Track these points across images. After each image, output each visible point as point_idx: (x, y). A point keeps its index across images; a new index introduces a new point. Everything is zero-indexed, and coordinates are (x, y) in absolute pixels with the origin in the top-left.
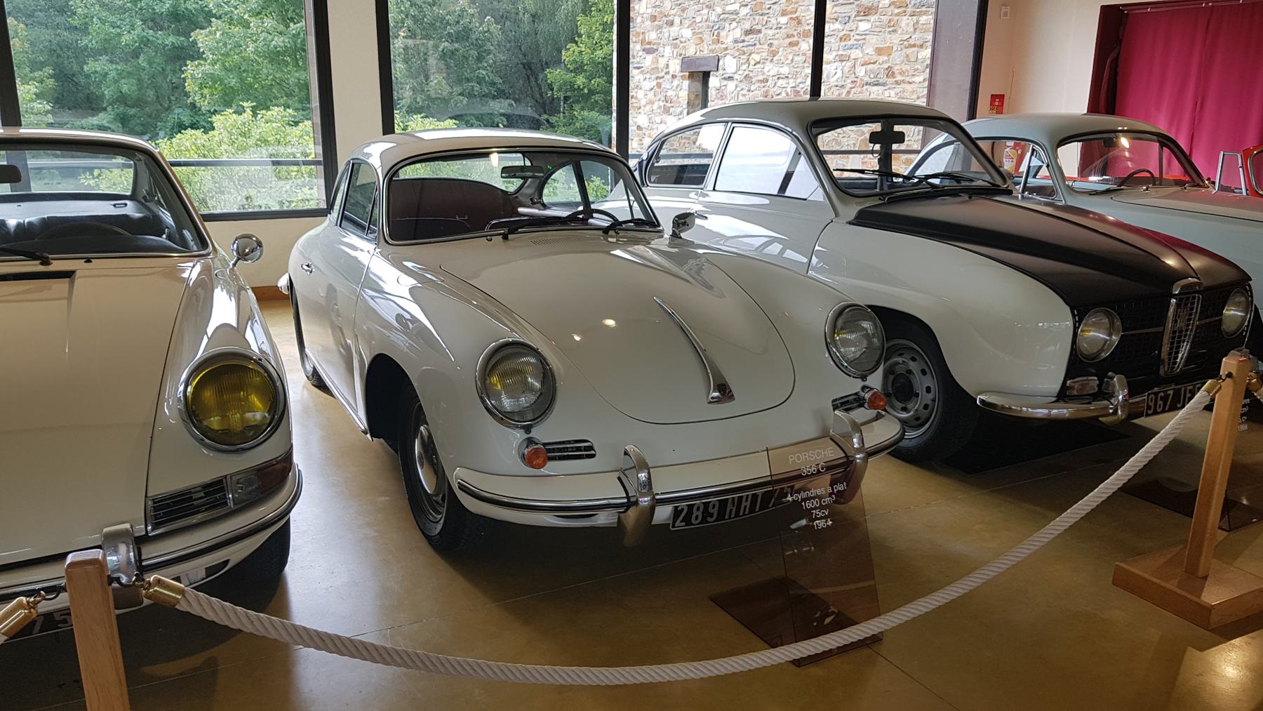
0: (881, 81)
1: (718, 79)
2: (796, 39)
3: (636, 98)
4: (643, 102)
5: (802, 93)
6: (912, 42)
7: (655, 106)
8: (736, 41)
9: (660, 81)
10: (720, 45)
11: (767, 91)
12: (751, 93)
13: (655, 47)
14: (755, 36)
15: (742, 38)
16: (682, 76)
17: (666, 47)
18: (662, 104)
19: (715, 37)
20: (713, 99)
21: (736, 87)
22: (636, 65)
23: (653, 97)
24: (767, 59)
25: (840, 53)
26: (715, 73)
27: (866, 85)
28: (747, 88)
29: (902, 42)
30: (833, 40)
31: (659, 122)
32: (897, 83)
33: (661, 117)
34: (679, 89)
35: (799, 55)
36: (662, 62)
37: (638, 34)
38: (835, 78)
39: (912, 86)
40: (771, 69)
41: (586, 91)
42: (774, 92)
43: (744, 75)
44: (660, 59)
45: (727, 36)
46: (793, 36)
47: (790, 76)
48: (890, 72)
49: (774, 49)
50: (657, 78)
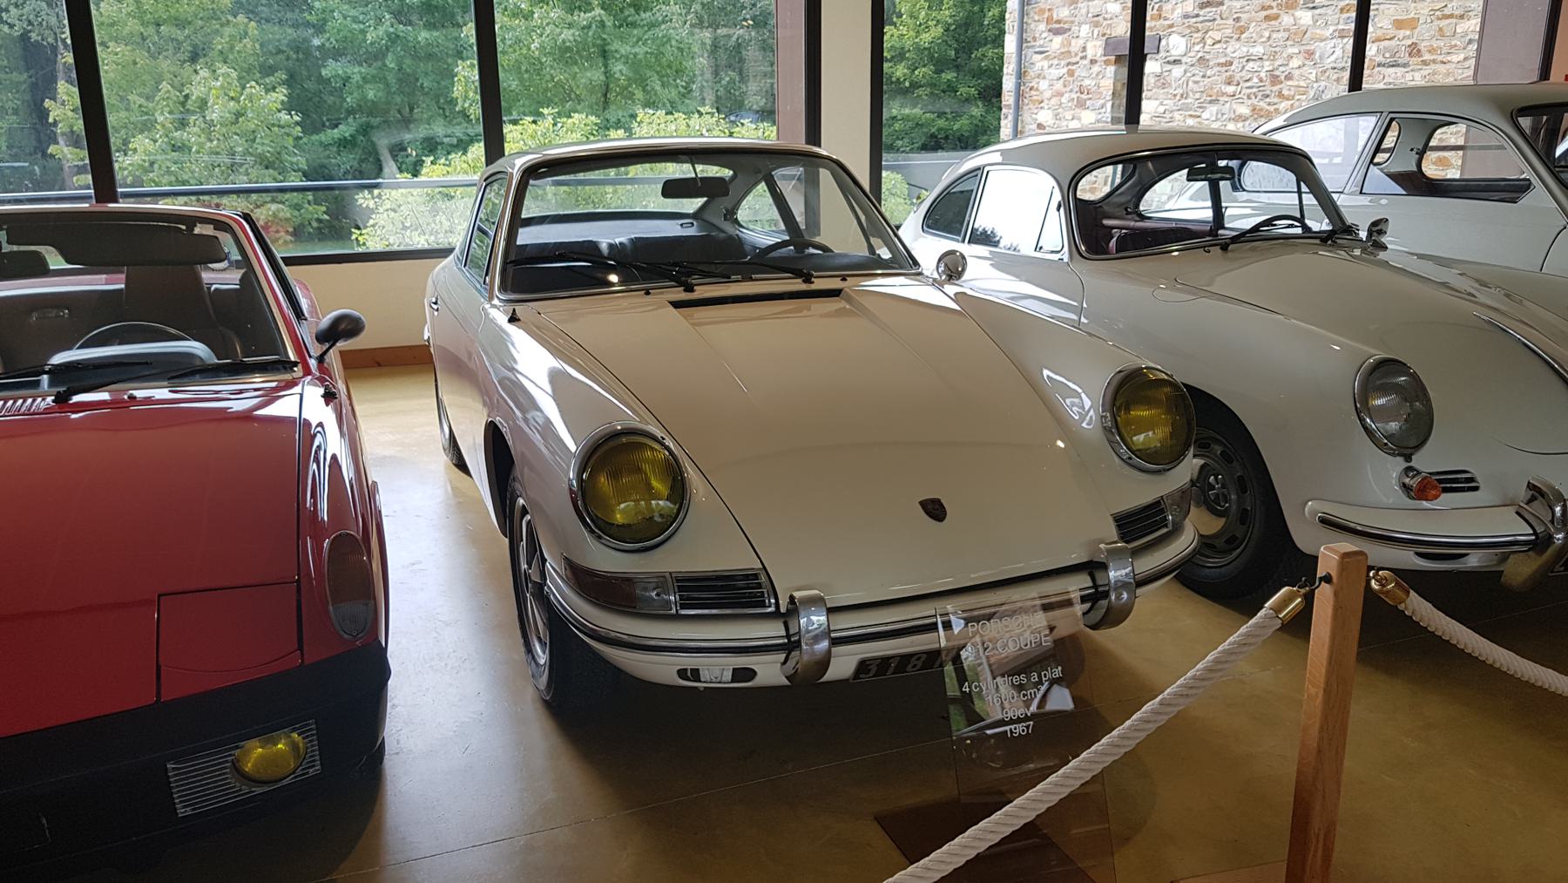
0: (1400, 61)
1: (1158, 64)
2: (1275, 11)
3: (1037, 90)
4: (1048, 94)
5: (1283, 78)
6: (1447, 11)
7: (1063, 100)
8: (1186, 16)
9: (1074, 67)
10: (1161, 21)
11: (1231, 77)
12: (1206, 80)
13: (1066, 26)
14: (1214, 9)
15: (1196, 12)
16: (1105, 62)
17: (1083, 26)
18: (1074, 96)
19: (1155, 11)
20: (1150, 88)
21: (1185, 72)
22: (1037, 50)
23: (1062, 87)
24: (1232, 37)
25: (1341, 27)
26: (1154, 56)
27: (1379, 65)
28: (1201, 74)
29: (1432, 13)
30: (1330, 11)
31: (1070, 118)
32: (1425, 63)
33: (1072, 112)
34: (1100, 77)
35: (1278, 31)
36: (1076, 45)
37: (1042, 11)
38: (1333, 58)
39: (1447, 66)
40: (1236, 49)
41: (907, 84)
42: (1241, 77)
43: (1199, 56)
44: (1074, 42)
45: (1173, 10)
46: (1271, 7)
47: (1265, 57)
48: (1414, 50)
49: (1242, 24)
50: (1068, 64)
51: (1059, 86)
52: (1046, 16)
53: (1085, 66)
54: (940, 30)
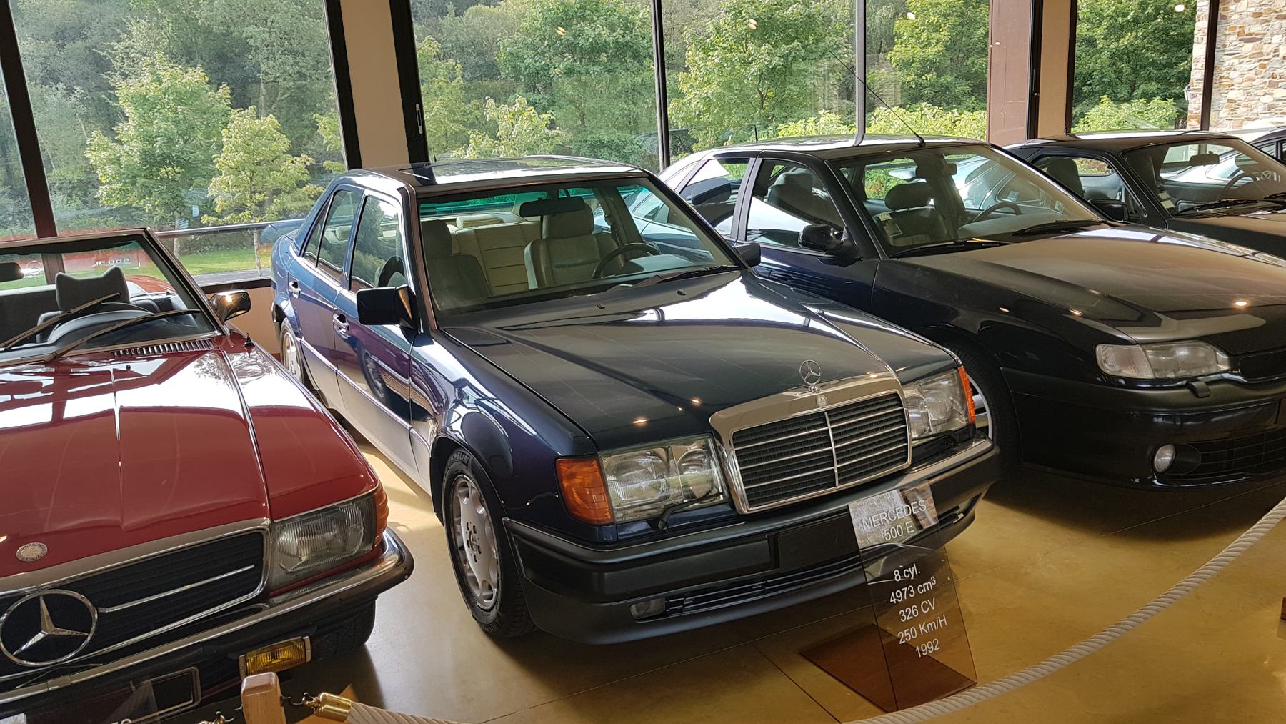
13: (1258, 37)
22: (1226, 53)
33: (1264, 90)
36: (1267, 49)
37: (1234, 28)
44: (1265, 46)
51: (1251, 75)
52: (1238, 30)
53: (1278, 61)
54: (940, 47)
